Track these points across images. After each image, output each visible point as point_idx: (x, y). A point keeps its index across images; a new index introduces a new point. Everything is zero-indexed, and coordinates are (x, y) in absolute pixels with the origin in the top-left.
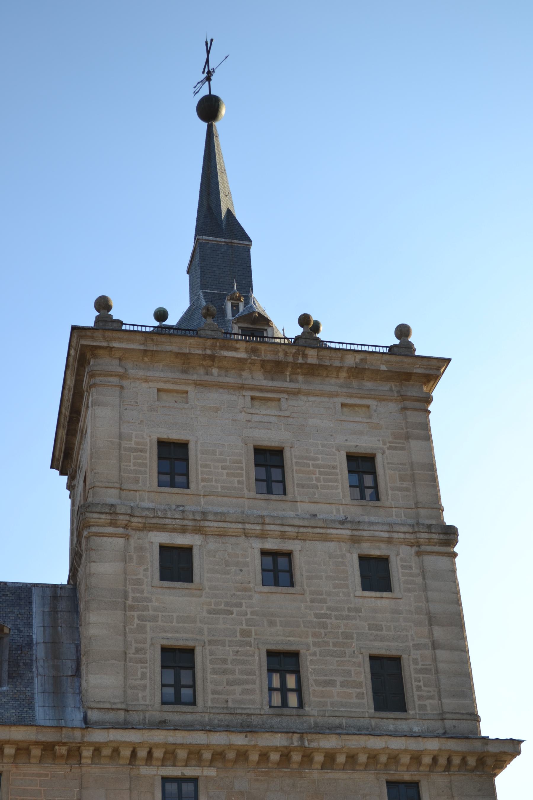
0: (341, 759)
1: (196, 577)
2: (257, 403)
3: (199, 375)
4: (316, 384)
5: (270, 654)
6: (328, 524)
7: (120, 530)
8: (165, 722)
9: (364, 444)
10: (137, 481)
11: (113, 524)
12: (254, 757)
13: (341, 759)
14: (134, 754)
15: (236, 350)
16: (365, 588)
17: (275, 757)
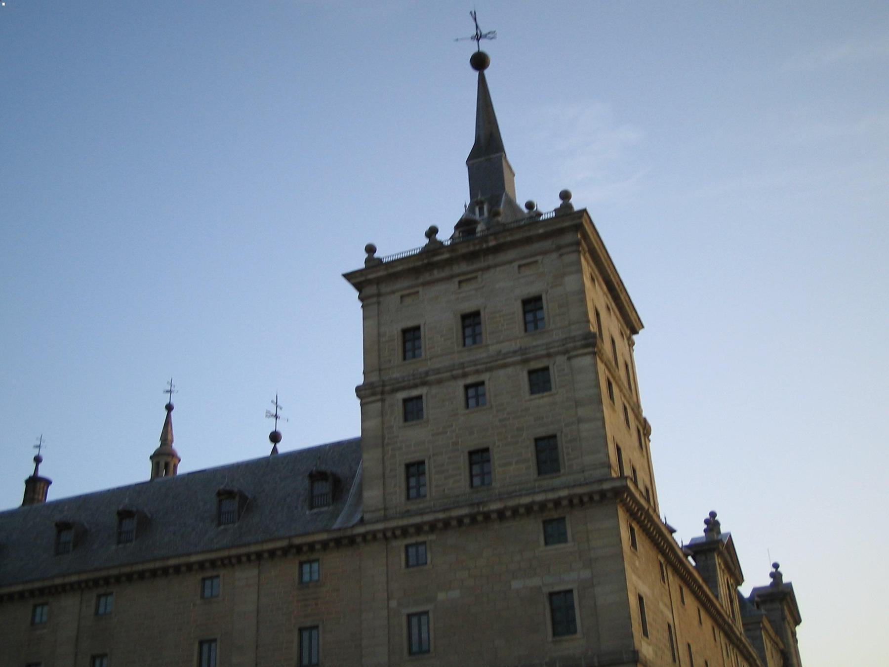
0: (508, 513)
1: (425, 417)
2: (464, 285)
3: (427, 277)
4: (503, 257)
5: (471, 453)
6: (506, 355)
7: (379, 397)
8: (408, 511)
9: (532, 290)
10: (390, 361)
11: (374, 394)
12: (454, 523)
13: (508, 513)
14: (385, 535)
15: (442, 254)
16: (532, 392)
17: (467, 521)
